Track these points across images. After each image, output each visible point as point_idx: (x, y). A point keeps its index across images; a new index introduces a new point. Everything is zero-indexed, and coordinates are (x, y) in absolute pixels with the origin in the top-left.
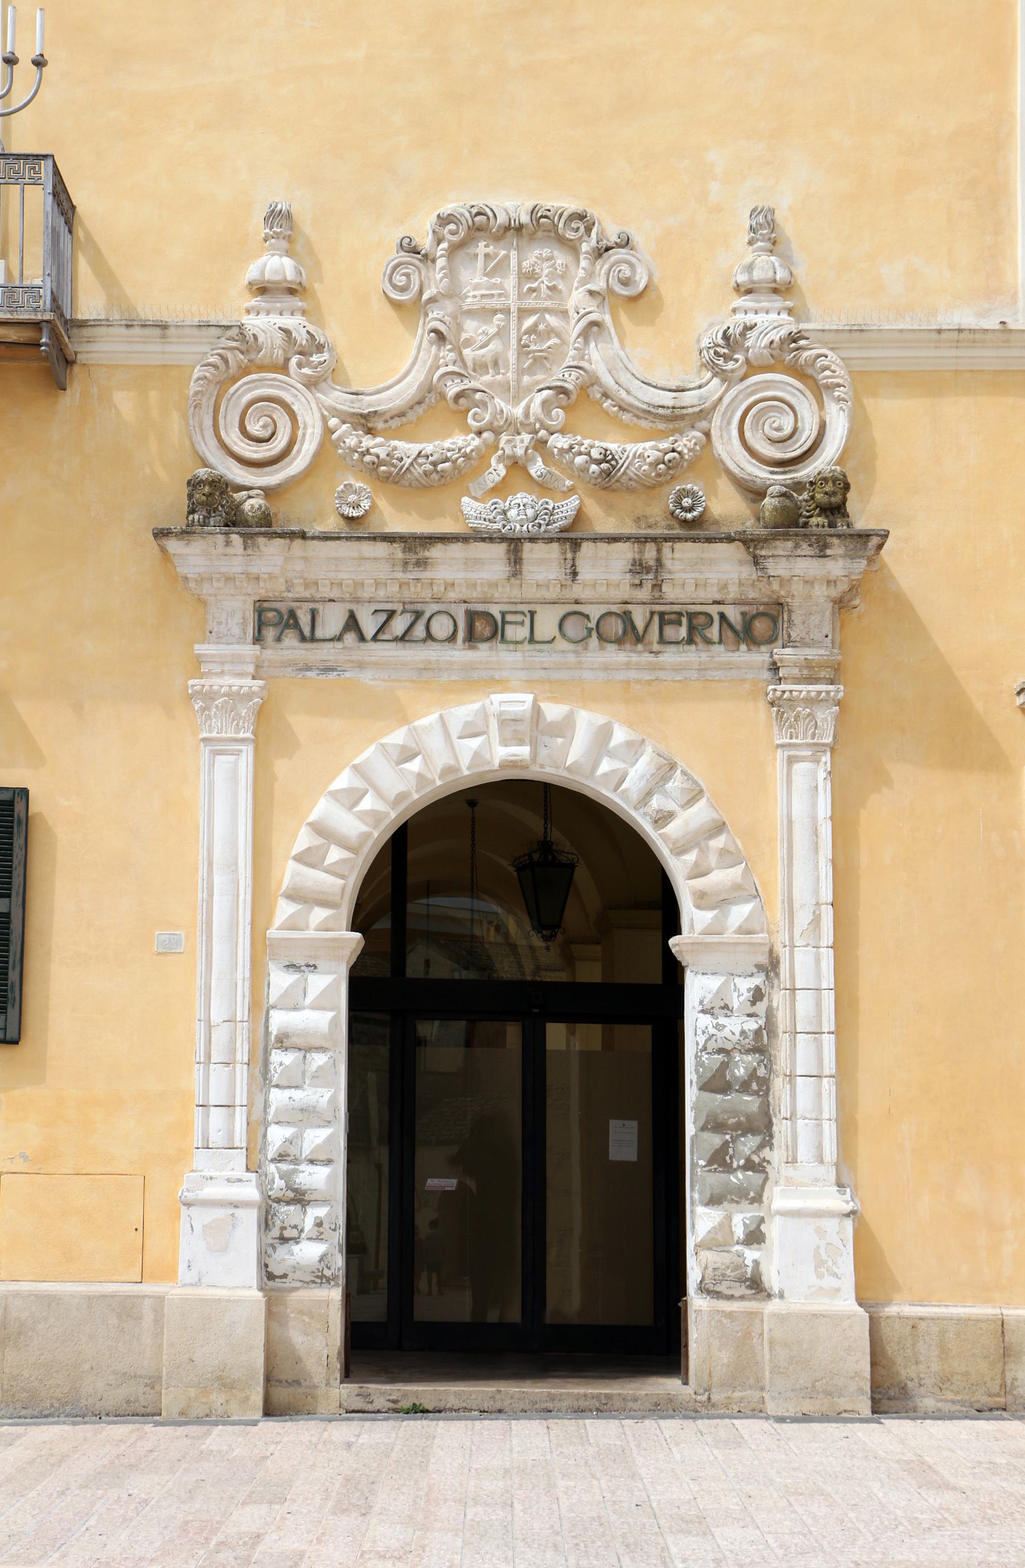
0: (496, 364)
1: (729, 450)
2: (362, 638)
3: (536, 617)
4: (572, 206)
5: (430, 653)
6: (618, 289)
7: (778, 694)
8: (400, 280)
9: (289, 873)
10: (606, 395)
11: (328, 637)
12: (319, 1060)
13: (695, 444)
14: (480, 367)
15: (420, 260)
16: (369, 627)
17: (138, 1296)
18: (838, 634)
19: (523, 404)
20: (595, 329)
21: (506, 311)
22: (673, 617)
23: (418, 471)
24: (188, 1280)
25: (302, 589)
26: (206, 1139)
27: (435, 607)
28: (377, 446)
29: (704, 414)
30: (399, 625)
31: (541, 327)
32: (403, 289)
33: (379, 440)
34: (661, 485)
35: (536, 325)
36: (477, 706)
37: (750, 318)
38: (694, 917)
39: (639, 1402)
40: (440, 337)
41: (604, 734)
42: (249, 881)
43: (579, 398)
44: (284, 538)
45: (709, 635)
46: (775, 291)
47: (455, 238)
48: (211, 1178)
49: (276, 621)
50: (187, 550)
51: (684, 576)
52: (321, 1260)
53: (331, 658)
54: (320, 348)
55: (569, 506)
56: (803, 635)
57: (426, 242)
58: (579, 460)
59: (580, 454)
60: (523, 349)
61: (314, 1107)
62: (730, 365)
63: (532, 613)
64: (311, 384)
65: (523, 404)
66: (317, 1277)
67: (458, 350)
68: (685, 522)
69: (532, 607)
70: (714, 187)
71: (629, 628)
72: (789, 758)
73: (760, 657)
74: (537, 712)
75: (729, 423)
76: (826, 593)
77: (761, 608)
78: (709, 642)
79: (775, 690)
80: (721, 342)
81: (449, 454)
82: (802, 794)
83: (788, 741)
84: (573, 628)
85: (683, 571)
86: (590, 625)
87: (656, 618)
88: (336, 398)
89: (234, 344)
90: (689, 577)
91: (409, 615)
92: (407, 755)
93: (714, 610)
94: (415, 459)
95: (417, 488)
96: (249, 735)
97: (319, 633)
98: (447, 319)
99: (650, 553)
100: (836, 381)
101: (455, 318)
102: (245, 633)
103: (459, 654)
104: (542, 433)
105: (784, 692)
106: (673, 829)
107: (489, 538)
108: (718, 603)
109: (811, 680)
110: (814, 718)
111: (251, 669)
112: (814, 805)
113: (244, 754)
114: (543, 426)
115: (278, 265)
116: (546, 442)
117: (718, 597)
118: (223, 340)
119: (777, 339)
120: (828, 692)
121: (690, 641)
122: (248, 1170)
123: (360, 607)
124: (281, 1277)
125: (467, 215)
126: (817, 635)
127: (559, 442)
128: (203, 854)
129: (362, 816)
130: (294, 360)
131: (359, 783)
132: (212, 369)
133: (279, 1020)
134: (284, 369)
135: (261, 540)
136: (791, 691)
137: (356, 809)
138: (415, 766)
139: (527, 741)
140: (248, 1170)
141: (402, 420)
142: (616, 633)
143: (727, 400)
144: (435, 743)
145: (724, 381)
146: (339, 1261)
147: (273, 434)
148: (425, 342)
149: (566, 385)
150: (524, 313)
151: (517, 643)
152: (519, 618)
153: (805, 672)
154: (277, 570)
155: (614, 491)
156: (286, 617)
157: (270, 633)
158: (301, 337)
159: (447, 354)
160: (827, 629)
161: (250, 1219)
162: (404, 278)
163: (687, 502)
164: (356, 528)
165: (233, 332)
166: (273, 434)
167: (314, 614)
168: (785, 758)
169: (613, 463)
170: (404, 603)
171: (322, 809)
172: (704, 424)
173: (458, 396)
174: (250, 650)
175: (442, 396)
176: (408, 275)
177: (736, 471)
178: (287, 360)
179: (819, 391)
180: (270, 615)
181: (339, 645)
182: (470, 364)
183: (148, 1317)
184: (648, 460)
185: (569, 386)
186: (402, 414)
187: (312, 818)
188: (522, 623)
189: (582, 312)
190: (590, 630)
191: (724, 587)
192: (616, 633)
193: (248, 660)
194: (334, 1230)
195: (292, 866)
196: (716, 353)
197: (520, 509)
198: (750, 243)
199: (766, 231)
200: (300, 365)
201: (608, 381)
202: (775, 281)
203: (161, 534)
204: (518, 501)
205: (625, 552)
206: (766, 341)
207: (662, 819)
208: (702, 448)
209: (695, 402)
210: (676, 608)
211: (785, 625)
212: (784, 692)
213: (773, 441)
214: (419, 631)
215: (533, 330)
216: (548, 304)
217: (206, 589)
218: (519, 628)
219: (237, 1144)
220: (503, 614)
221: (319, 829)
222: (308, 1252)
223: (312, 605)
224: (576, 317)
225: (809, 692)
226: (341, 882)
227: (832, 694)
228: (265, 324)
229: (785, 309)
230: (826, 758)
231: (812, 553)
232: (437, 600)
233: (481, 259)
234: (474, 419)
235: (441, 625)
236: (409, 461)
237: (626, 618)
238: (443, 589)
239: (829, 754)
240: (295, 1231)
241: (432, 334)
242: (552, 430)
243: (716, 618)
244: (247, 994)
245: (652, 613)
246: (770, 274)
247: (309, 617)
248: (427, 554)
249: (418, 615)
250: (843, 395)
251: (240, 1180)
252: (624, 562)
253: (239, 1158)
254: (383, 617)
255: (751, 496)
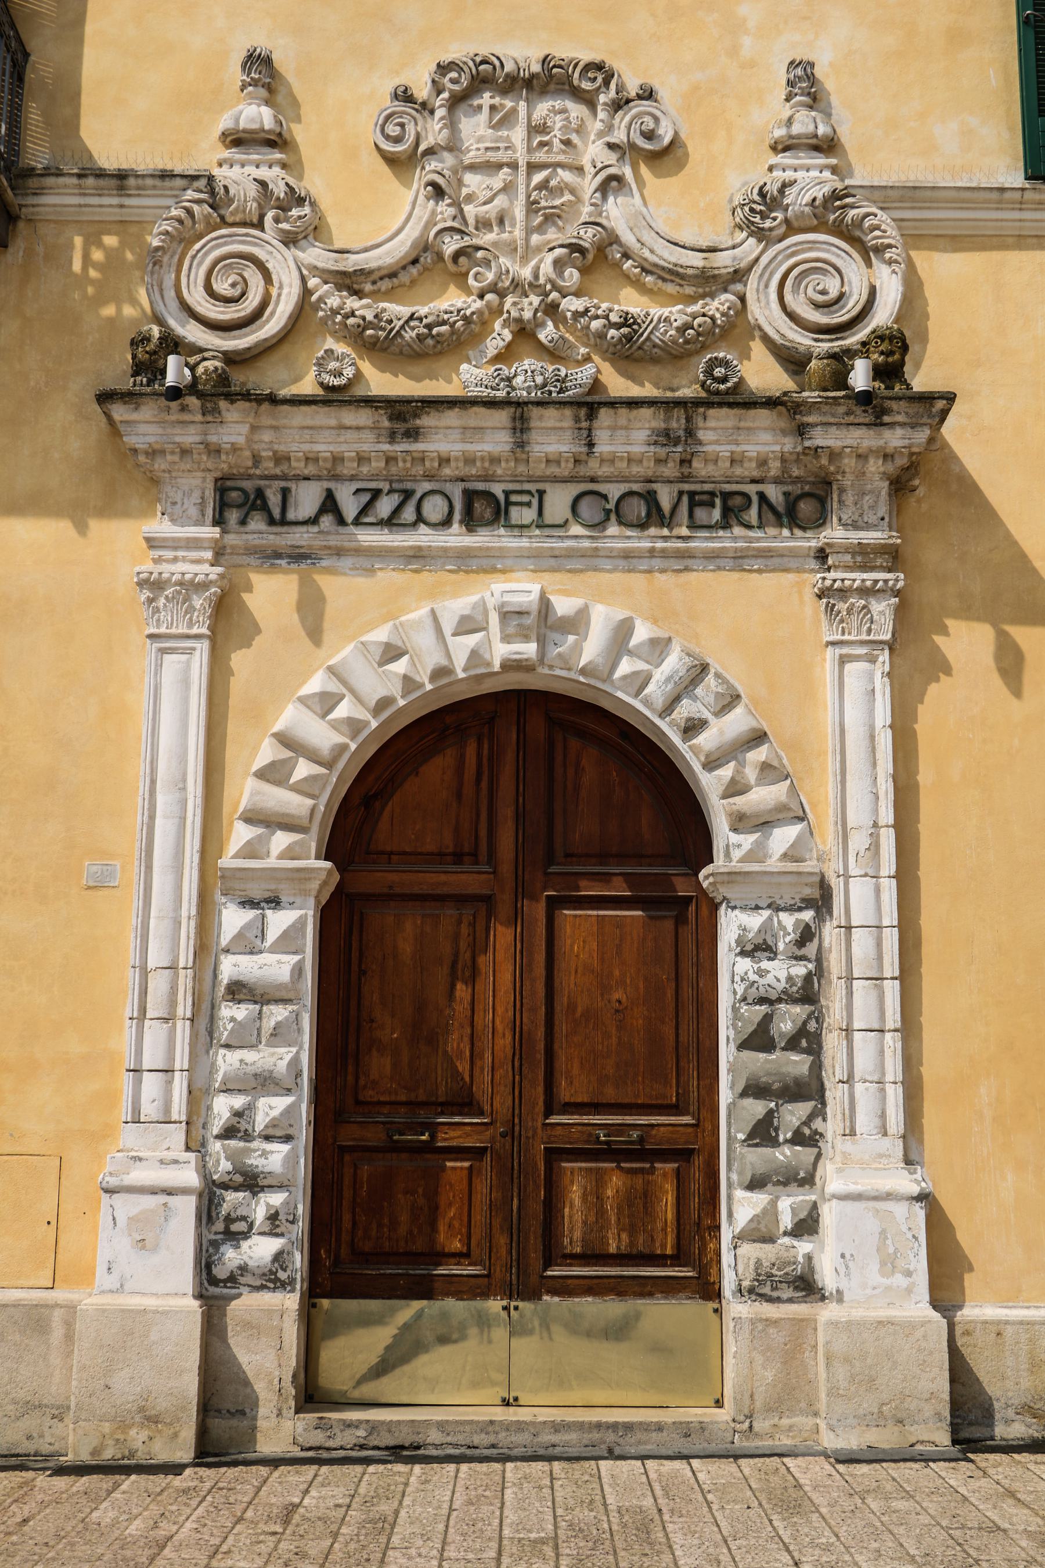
0: (501, 221)
1: (765, 312)
2: (341, 521)
3: (547, 499)
4: (586, 56)
5: (424, 537)
6: (641, 142)
7: (828, 583)
8: (393, 130)
9: (244, 790)
10: (626, 256)
11: (301, 519)
12: (278, 1013)
13: (729, 308)
14: (484, 224)
15: (417, 110)
16: (350, 508)
17: (47, 1306)
18: (894, 519)
19: (533, 263)
20: (614, 184)
21: (514, 166)
22: (705, 497)
23: (409, 335)
24: (107, 1286)
25: (271, 465)
26: (136, 1109)
27: (427, 486)
28: (362, 308)
29: (739, 275)
30: (385, 507)
31: (553, 183)
32: (397, 140)
33: (365, 301)
34: (690, 354)
35: (547, 181)
36: (474, 598)
37: (789, 175)
38: (730, 846)
39: (665, 1434)
40: (438, 192)
41: (623, 630)
42: (199, 801)
43: (598, 257)
44: (250, 400)
45: (746, 518)
46: (817, 148)
47: (456, 87)
48: (140, 1159)
49: (240, 501)
50: (135, 416)
51: (718, 448)
52: (279, 1257)
53: (304, 543)
54: (300, 201)
55: (584, 374)
56: (856, 517)
57: (422, 91)
58: (596, 325)
59: (597, 317)
60: (532, 206)
61: (271, 1072)
62: (768, 224)
63: (541, 493)
64: (290, 240)
65: (533, 263)
66: (270, 1280)
67: (456, 204)
68: (718, 393)
69: (541, 486)
70: (747, 41)
71: (654, 510)
72: (841, 656)
73: (808, 541)
74: (545, 604)
75: (767, 286)
76: (882, 469)
77: (807, 488)
78: (749, 527)
79: (824, 579)
80: (757, 198)
81: (446, 317)
82: (855, 698)
83: (839, 637)
84: (586, 508)
85: (717, 442)
86: (608, 507)
87: (685, 499)
88: (314, 255)
89: (202, 196)
90: (724, 450)
91: (396, 496)
92: (391, 653)
93: (751, 489)
94: (407, 322)
95: (409, 356)
96: (204, 631)
97: (291, 516)
98: (446, 172)
99: (677, 423)
100: (886, 241)
101: (455, 172)
102: (203, 515)
103: (456, 538)
104: (554, 295)
105: (835, 581)
106: (706, 740)
107: (491, 404)
108: (754, 481)
109: (864, 568)
110: (869, 611)
111: (209, 555)
112: (871, 711)
113: (197, 653)
114: (555, 287)
115: (257, 115)
116: (558, 305)
117: (756, 474)
118: (189, 192)
119: (820, 196)
120: (886, 581)
121: (725, 525)
122: (188, 1149)
123: (339, 486)
124: (225, 1281)
125: (471, 64)
126: (872, 518)
127: (572, 304)
128: (144, 768)
129: (335, 725)
130: (270, 216)
131: (334, 687)
132: (176, 224)
133: (232, 967)
134: (260, 225)
135: (223, 404)
136: (843, 580)
137: (329, 717)
138: (400, 667)
139: (534, 637)
140: (188, 1149)
141: (391, 280)
142: (639, 516)
143: (764, 260)
144: (424, 641)
145: (760, 241)
146: (298, 1260)
147: (243, 294)
148: (421, 198)
149: (581, 242)
150: (533, 168)
151: (522, 527)
152: (525, 498)
153: (859, 559)
154: (241, 440)
155: (636, 360)
156: (252, 497)
157: (233, 516)
158: (279, 190)
159: (445, 210)
160: (883, 510)
161: (186, 1208)
162: (398, 128)
163: (719, 372)
164: (335, 396)
165: (202, 183)
166: (243, 294)
167: (285, 493)
168: (837, 657)
169: (635, 327)
170: (391, 482)
171: (290, 717)
172: (739, 287)
173: (457, 256)
174: (212, 532)
175: (440, 256)
176: (402, 125)
177: (776, 337)
178: (262, 217)
179: (869, 253)
180: (234, 494)
181: (315, 529)
182: (471, 221)
183: (58, 1332)
184: (675, 324)
185: (586, 245)
186: (393, 275)
187: (276, 729)
188: (529, 504)
189: (599, 165)
190: (608, 512)
191: (763, 463)
192: (639, 516)
193: (206, 545)
194: (292, 1222)
195: (251, 784)
196: (752, 210)
197: (527, 373)
198: (787, 100)
199: (805, 84)
200: (277, 220)
201: (628, 238)
202: (816, 136)
203: (105, 398)
204: (526, 367)
205: (647, 421)
206: (807, 198)
207: (692, 728)
208: (737, 313)
209: (728, 262)
210: (707, 487)
211: (835, 505)
212: (835, 581)
213: (817, 306)
214: (409, 514)
215: (544, 185)
216: (561, 158)
217: (160, 464)
218: (525, 510)
219: (175, 1117)
220: (507, 493)
221: (284, 740)
222: (260, 1250)
223: (283, 484)
224: (593, 171)
225: (863, 581)
226: (310, 802)
227: (891, 583)
228: (241, 176)
229: (827, 167)
230: (885, 656)
231: (867, 420)
232: (429, 477)
233: (486, 110)
234: (476, 280)
235: (435, 506)
236: (401, 322)
237: (650, 498)
238: (436, 464)
239: (887, 652)
240: (243, 1223)
241: (429, 188)
242: (564, 292)
243: (755, 499)
244: (192, 935)
245: (681, 493)
246: (811, 128)
247: (279, 497)
248: (418, 422)
249: (408, 494)
250: (895, 257)
251: (176, 1162)
252: (648, 432)
253: (177, 1135)
254: (366, 498)
255: (792, 367)
